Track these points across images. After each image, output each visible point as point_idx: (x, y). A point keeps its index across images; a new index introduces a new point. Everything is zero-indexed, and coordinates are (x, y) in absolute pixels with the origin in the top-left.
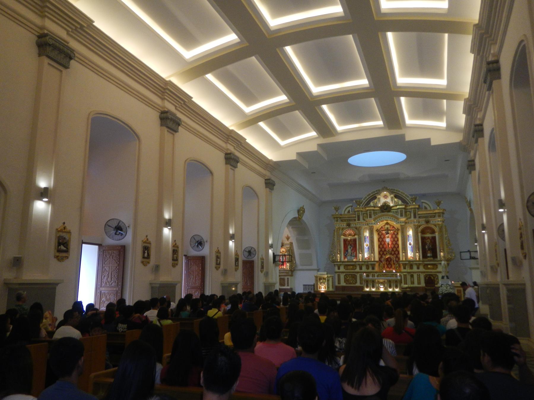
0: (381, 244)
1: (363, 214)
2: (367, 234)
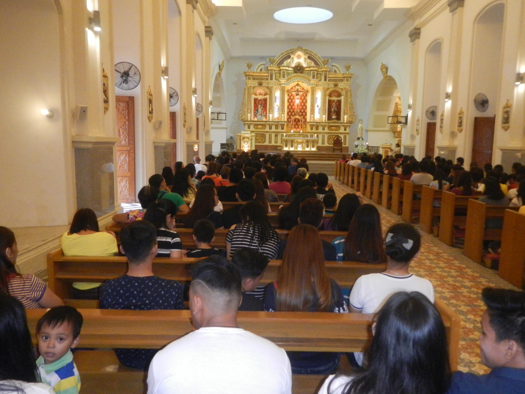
0: (290, 105)
1: (276, 73)
2: (277, 94)
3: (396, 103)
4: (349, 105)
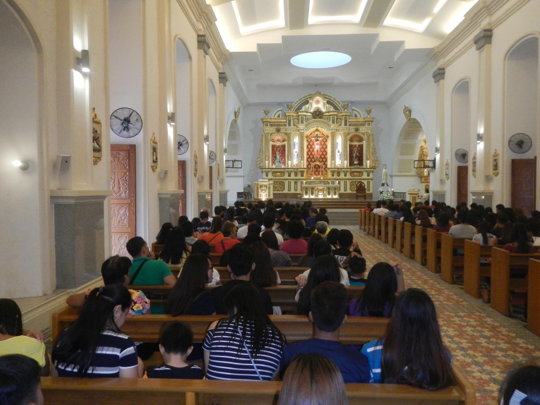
0: (309, 151)
1: (294, 119)
3: (421, 147)
4: (371, 150)
